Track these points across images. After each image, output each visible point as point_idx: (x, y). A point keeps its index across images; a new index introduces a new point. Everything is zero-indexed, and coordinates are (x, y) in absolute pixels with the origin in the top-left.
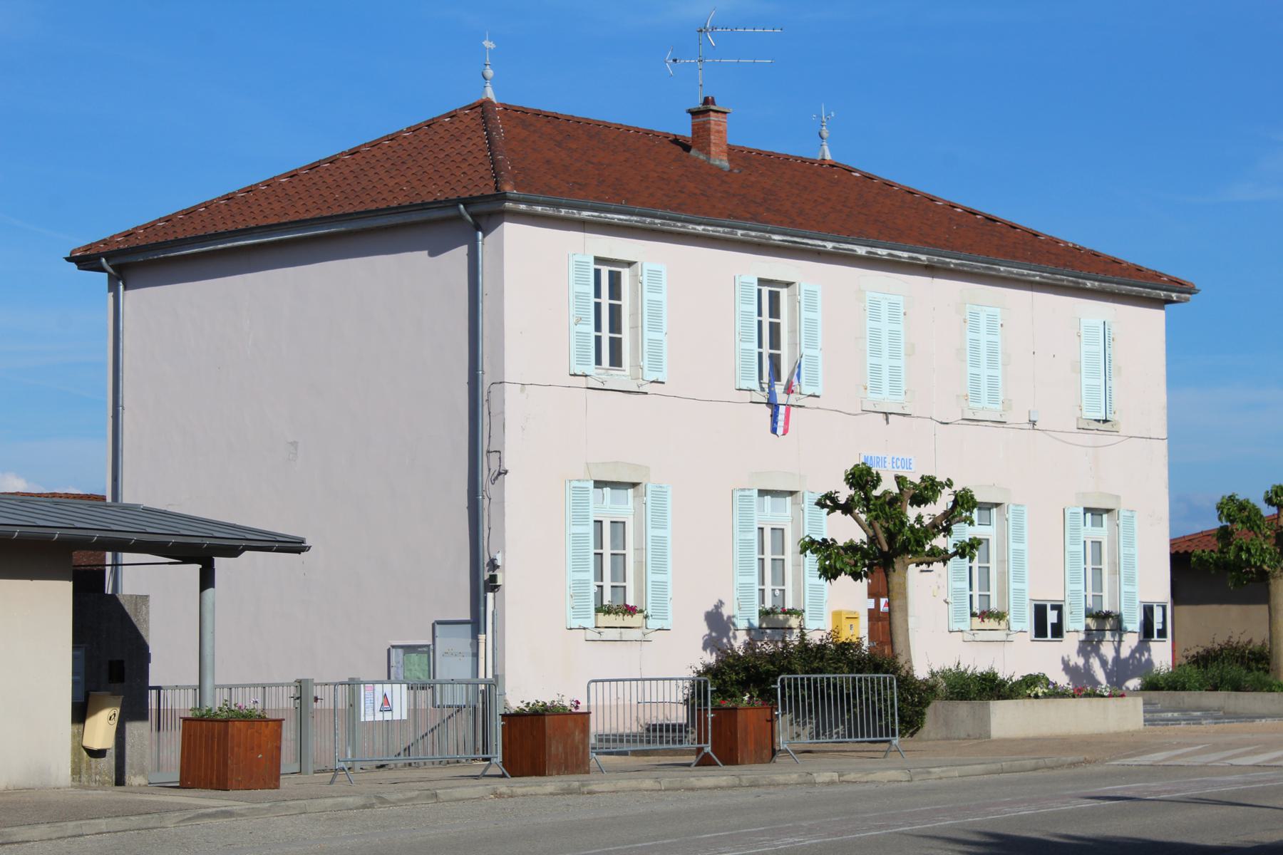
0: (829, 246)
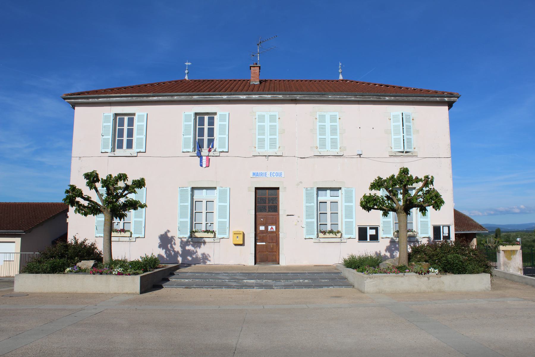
0: (225, 97)
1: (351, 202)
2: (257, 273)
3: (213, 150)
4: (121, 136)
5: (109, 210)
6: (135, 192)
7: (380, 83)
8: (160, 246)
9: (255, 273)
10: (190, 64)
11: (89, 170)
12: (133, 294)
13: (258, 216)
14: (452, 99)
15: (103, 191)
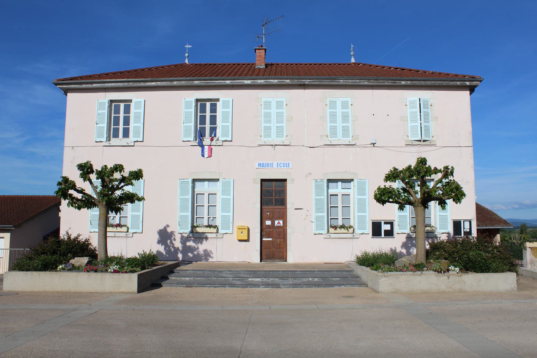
0: (228, 82)
1: (364, 194)
2: (263, 271)
3: (215, 139)
4: (117, 124)
5: (104, 203)
6: (132, 184)
7: (395, 66)
8: (159, 242)
9: (261, 271)
10: (190, 46)
11: (84, 161)
12: (130, 293)
13: (264, 210)
14: (474, 83)
15: (98, 183)
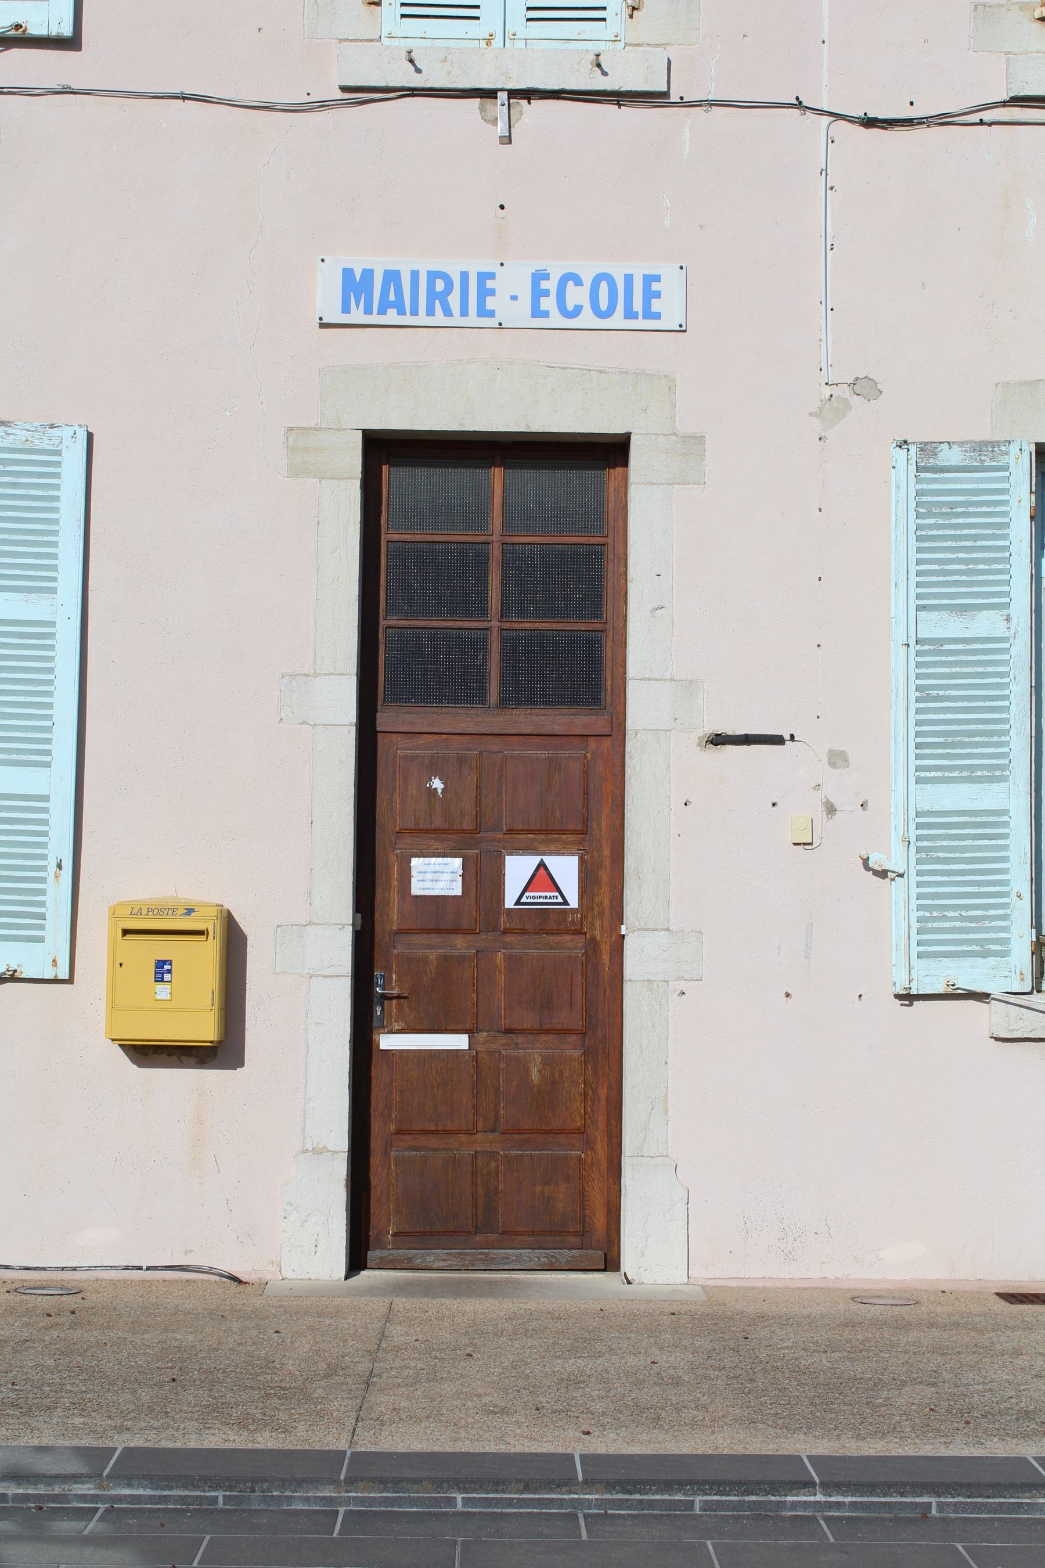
2: (370, 1469)
9: (320, 1465)
13: (391, 750)
